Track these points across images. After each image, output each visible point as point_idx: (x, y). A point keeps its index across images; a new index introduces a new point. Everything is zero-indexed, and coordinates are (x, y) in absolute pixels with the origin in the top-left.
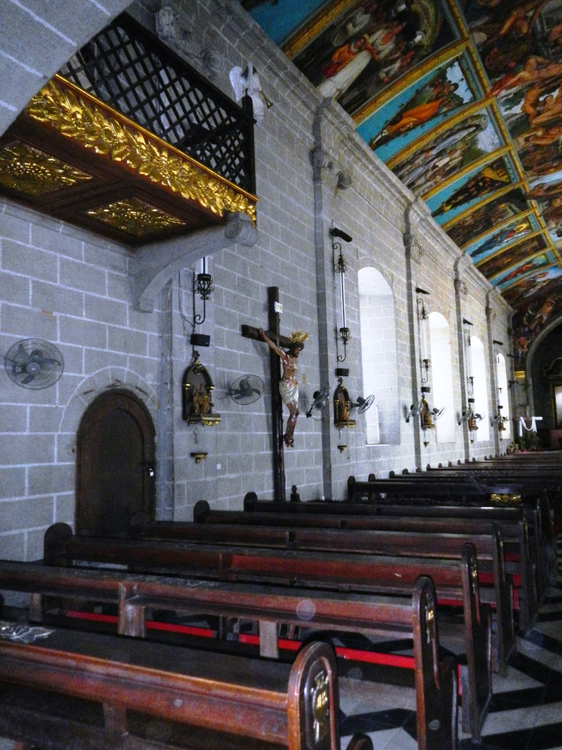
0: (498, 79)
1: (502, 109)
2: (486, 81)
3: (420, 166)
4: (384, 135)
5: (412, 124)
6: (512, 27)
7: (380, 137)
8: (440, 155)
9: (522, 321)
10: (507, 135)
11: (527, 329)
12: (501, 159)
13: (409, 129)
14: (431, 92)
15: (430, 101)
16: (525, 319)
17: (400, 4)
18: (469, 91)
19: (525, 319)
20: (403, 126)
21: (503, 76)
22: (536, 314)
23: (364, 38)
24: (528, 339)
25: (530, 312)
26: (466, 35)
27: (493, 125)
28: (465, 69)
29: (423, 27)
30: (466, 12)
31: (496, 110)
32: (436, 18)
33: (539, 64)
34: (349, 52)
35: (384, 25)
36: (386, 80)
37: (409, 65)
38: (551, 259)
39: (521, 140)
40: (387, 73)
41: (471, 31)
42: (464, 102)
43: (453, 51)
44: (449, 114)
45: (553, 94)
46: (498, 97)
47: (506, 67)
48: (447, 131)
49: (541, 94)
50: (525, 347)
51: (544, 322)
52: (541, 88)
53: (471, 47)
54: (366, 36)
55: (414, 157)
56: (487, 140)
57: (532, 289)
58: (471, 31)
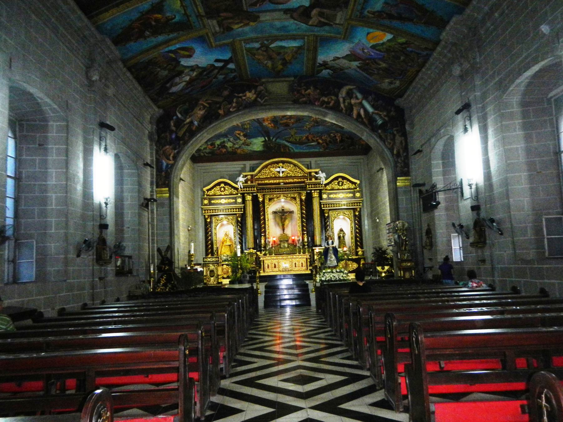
9: (169, 126)
11: (174, 136)
16: (172, 124)
19: (172, 124)
22: (186, 118)
24: (175, 149)
25: (179, 116)
38: (193, 19)
50: (171, 158)
51: (194, 128)
57: (177, 80)
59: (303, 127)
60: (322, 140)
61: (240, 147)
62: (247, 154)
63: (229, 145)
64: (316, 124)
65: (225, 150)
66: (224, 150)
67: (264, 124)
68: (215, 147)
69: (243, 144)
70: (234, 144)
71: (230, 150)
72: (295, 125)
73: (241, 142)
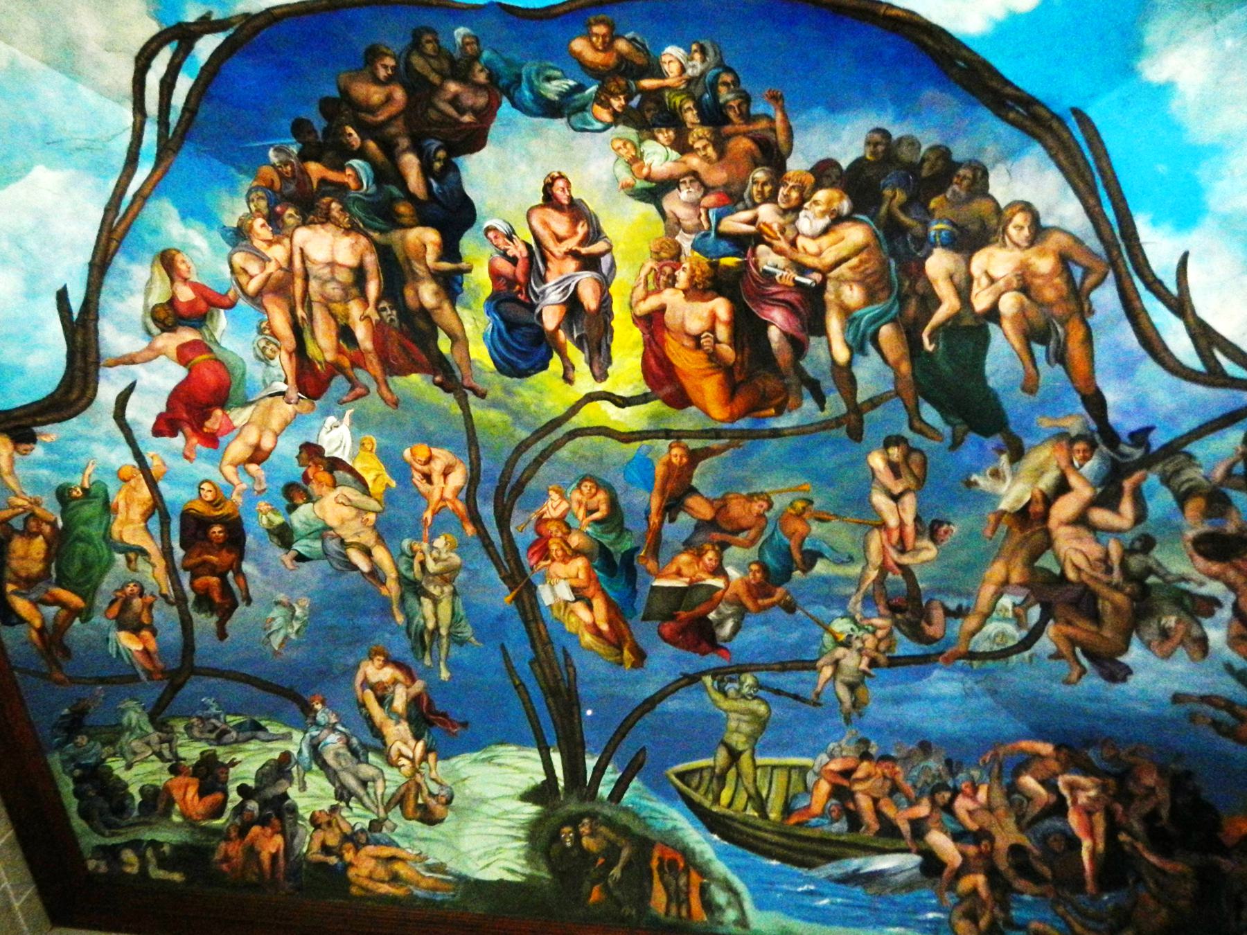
59: (811, 666)
60: (957, 837)
61: (376, 825)
62: (412, 898)
63: (311, 795)
64: (905, 646)
65: (279, 840)
66: (272, 844)
67: (546, 596)
68: (218, 812)
69: (399, 800)
70: (344, 794)
71: (308, 843)
72: (754, 638)
73: (394, 779)
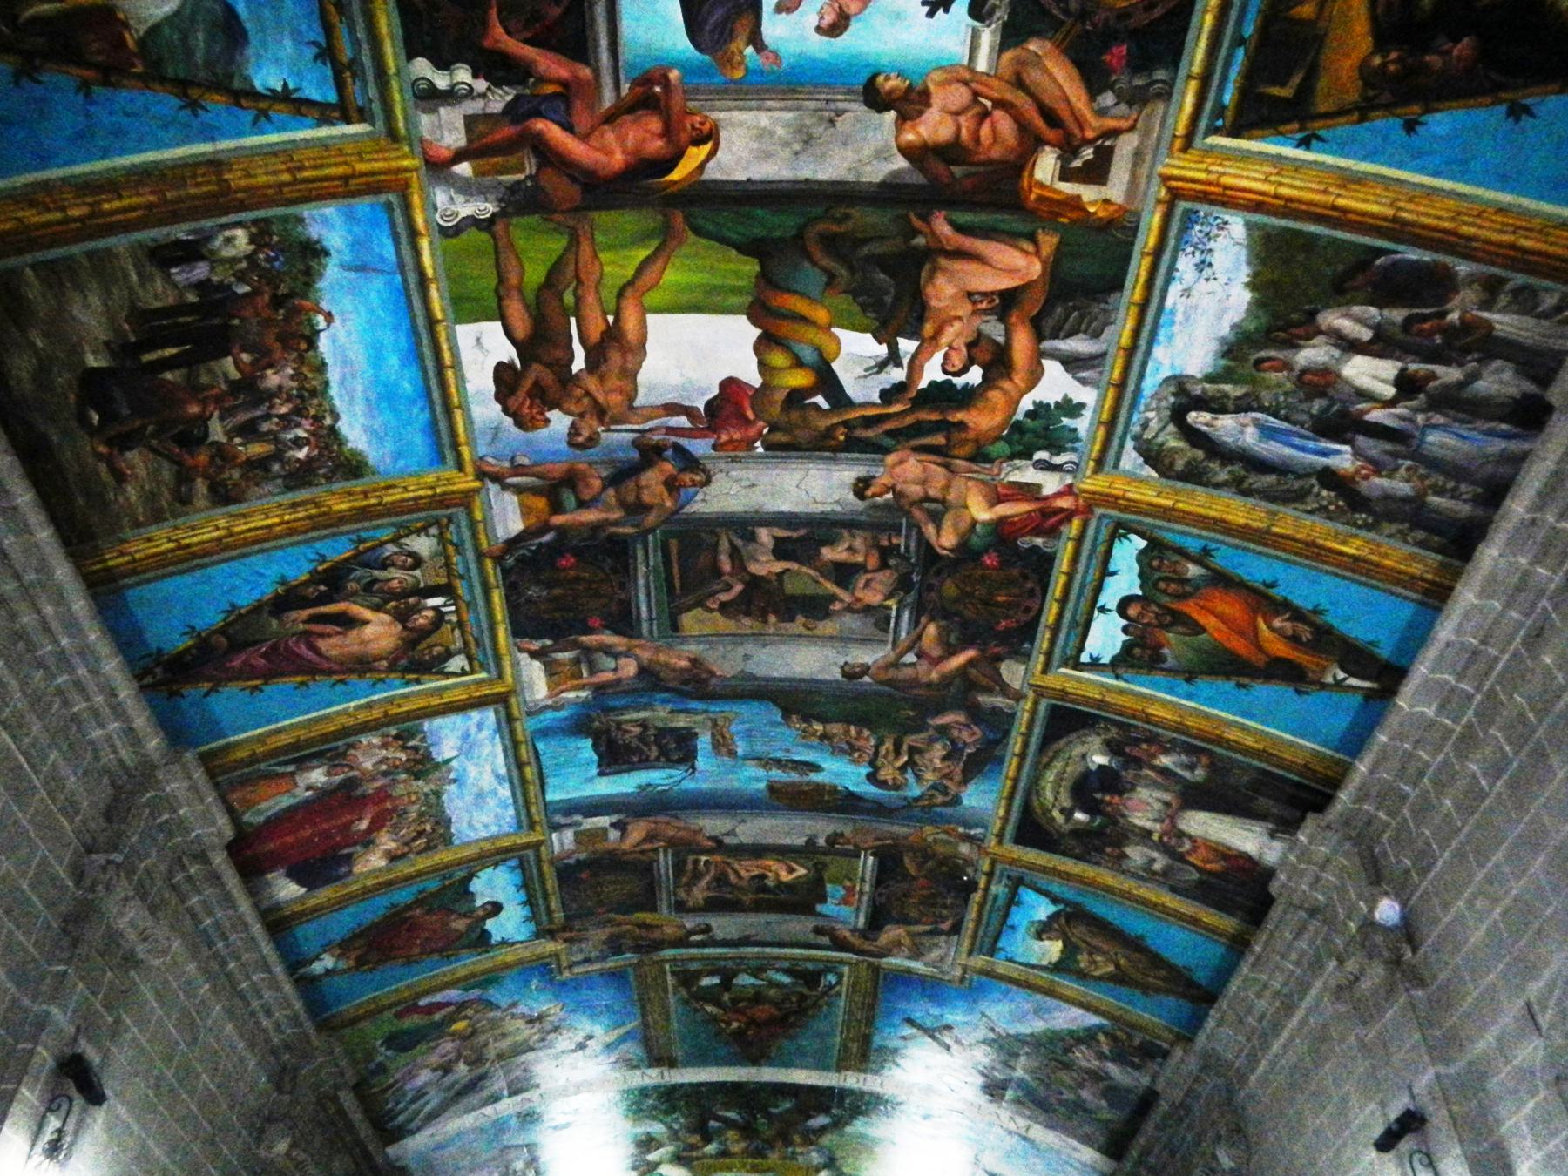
0: (1039, 541)
1: (1082, 424)
2: (1063, 564)
3: (1420, 457)
4: (1341, 675)
5: (1277, 623)
6: (951, 651)
7: (1353, 681)
8: (1341, 423)
10: (1139, 267)
12: (1253, 116)
13: (1297, 615)
14: (1174, 645)
15: (1199, 629)
17: (1079, 822)
18: (1112, 568)
20: (1294, 639)
21: (1025, 542)
23: (1161, 838)
26: (1031, 695)
27: (1141, 376)
28: (1080, 629)
29: (1080, 769)
30: (1007, 733)
31: (1101, 432)
32: (1052, 760)
33: (937, 518)
34: (1195, 849)
35: (1121, 820)
36: (1204, 760)
37: (1152, 739)
39: (1116, 189)
40: (1191, 767)
41: (1019, 697)
42: (1143, 544)
43: (1070, 686)
44: (1193, 545)
45: (940, 377)
46: (1069, 480)
47: (1004, 564)
48: (1246, 493)
49: (968, 397)
52: (961, 426)
53: (1039, 667)
54: (1156, 837)
55: (1391, 517)
56: (1205, 303)
58: (1019, 697)
